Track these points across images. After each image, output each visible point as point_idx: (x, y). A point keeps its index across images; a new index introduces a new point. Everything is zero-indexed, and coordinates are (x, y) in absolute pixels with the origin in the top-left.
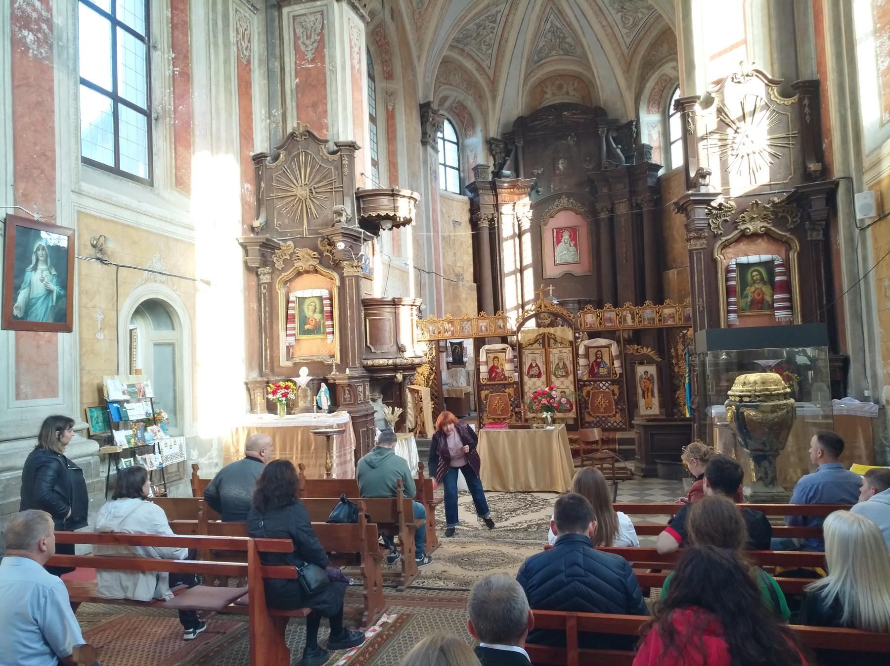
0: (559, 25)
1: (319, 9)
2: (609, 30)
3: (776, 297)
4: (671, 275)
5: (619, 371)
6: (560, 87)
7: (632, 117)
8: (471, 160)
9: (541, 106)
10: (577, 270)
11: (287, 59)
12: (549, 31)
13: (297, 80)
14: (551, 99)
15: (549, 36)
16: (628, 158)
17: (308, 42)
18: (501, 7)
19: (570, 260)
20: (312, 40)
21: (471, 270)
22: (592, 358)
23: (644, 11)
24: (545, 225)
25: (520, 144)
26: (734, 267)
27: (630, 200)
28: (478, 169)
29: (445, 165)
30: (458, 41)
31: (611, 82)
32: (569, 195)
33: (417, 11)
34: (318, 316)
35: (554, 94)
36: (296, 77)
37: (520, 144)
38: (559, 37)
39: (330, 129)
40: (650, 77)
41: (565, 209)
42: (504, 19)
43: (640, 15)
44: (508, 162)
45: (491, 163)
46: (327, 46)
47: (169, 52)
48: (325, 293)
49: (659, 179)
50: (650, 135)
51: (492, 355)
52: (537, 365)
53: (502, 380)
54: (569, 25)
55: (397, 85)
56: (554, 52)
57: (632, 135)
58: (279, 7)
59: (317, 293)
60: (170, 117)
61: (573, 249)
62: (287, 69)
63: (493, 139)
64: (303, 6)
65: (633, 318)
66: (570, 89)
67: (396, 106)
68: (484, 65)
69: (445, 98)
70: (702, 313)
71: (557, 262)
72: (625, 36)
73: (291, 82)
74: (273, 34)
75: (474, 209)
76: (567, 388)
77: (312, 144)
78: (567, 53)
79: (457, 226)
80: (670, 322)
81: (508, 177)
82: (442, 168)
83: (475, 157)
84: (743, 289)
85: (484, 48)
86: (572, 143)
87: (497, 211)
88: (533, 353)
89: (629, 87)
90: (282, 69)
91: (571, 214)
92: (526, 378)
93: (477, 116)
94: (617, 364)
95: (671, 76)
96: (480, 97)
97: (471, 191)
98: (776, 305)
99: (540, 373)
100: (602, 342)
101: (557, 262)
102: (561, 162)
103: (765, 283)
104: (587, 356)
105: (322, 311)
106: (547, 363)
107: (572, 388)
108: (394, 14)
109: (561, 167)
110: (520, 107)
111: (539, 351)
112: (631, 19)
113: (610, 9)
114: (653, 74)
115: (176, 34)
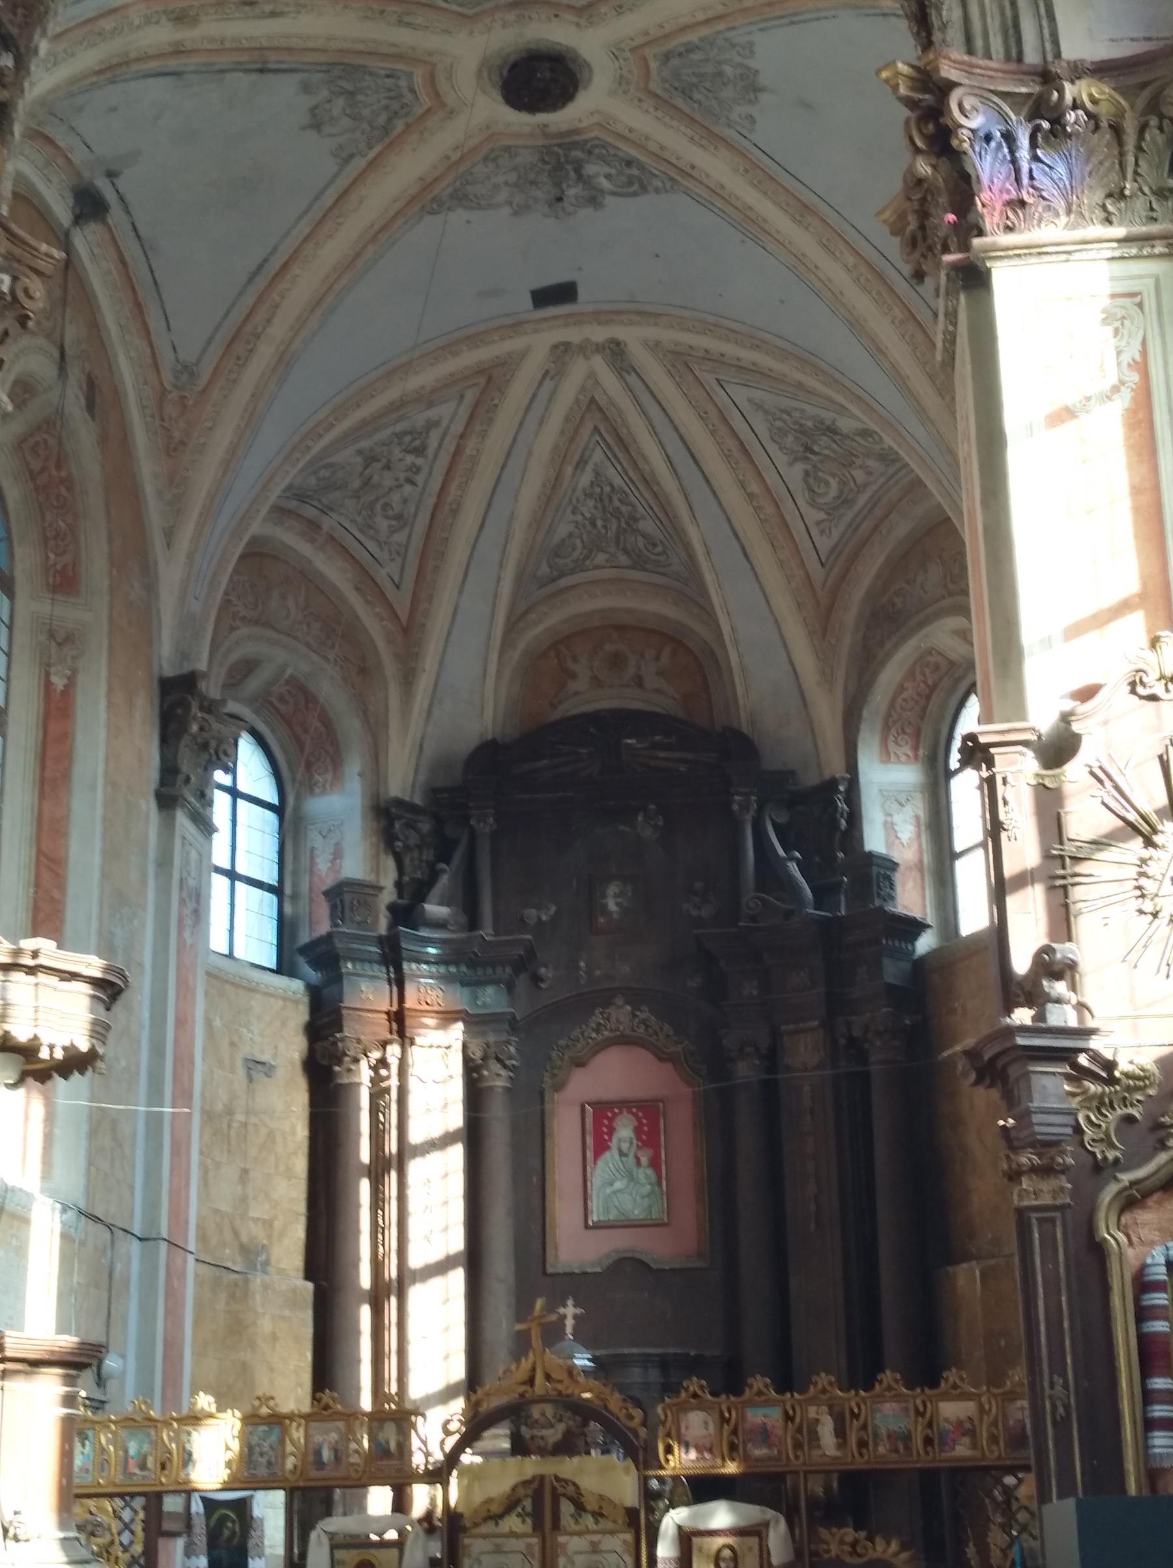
4: (961, 1281)
6: (617, 662)
8: (323, 865)
9: (557, 715)
10: (661, 1249)
12: (588, 495)
14: (586, 697)
15: (588, 508)
16: (823, 894)
18: (443, 411)
19: (637, 1213)
21: (299, 1231)
23: (872, 463)
24: (559, 1087)
25: (486, 826)
28: (344, 897)
29: (232, 875)
30: (299, 494)
33: (175, 395)
35: (597, 682)
37: (486, 826)
38: (617, 514)
41: (623, 1040)
42: (450, 446)
43: (859, 475)
44: (444, 880)
45: (388, 878)
49: (920, 965)
50: (890, 827)
54: (649, 481)
55: (91, 612)
56: (601, 558)
57: (834, 823)
61: (645, 1174)
63: (399, 802)
67: (81, 679)
69: (247, 667)
71: (594, 1217)
78: (639, 563)
79: (258, 1076)
80: (962, 1450)
81: (440, 925)
82: (220, 884)
83: (337, 854)
85: (383, 524)
86: (648, 833)
91: (643, 1056)
95: (954, 656)
97: (315, 964)
101: (594, 1217)
108: (99, 396)
109: (612, 906)
110: (489, 712)
112: (833, 483)
113: (772, 448)
114: (897, 646)
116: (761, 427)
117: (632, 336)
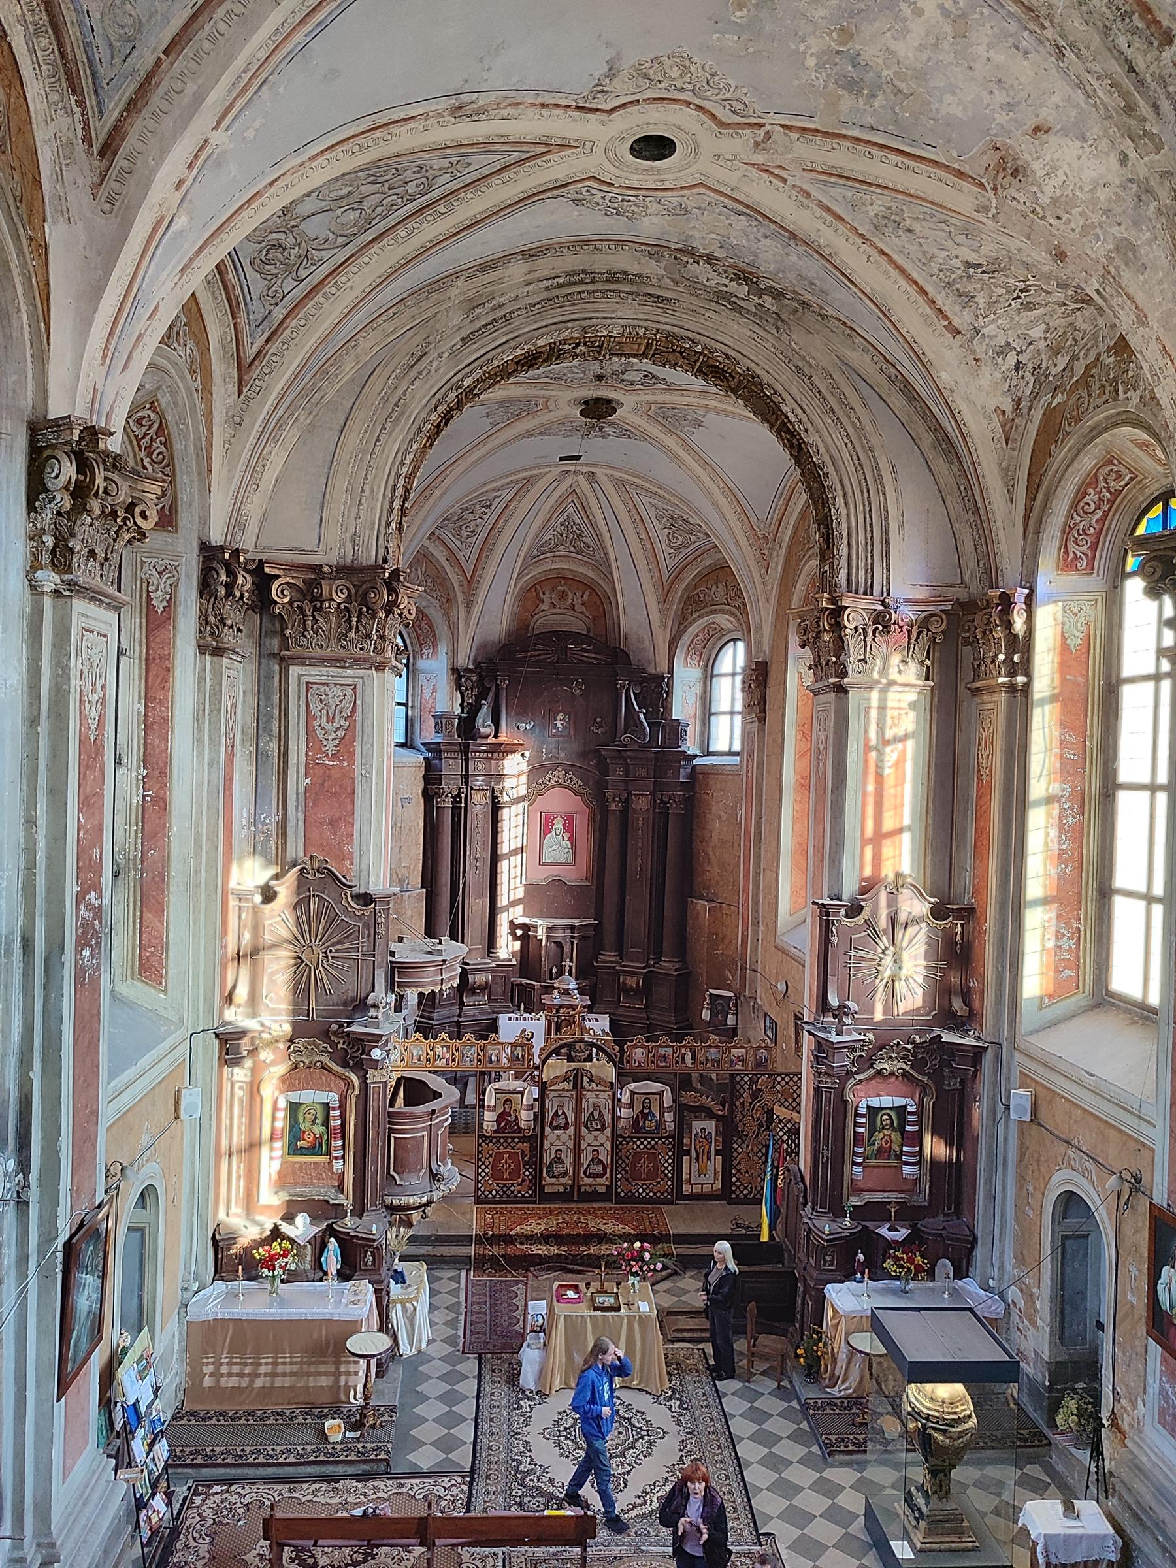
0: (577, 521)
1: (350, 681)
2: (649, 546)
3: (905, 1148)
5: (670, 1126)
6: (563, 596)
7: (663, 668)
11: (292, 746)
13: (308, 781)
17: (328, 727)
19: (562, 860)
20: (336, 725)
22: (638, 1108)
26: (864, 1110)
27: (653, 794)
31: (639, 612)
32: (567, 768)
34: (319, 1130)
36: (306, 775)
39: (356, 861)
40: (694, 621)
41: (561, 786)
46: (358, 739)
47: (139, 767)
48: (333, 1099)
51: (504, 1097)
52: (564, 1113)
53: (514, 1132)
58: (285, 662)
59: (323, 1097)
60: (135, 869)
62: (292, 760)
64: (324, 671)
65: (693, 1058)
66: (578, 602)
68: (460, 555)
70: (825, 1164)
72: (667, 557)
73: (297, 782)
74: (268, 698)
75: (432, 777)
76: (602, 1145)
77: (331, 886)
78: (579, 552)
84: (871, 1135)
87: (467, 784)
88: (560, 1096)
89: (664, 625)
90: (284, 754)
92: (547, 1129)
93: (442, 629)
94: (669, 1117)
96: (448, 601)
98: (905, 1158)
99: (567, 1123)
100: (656, 1086)
102: (560, 717)
103: (894, 1130)
104: (630, 1106)
105: (326, 1123)
106: (578, 1110)
107: (608, 1145)
109: (559, 725)
110: (504, 622)
111: (568, 1094)
115: (150, 738)
116: (652, 513)
117: (600, 473)
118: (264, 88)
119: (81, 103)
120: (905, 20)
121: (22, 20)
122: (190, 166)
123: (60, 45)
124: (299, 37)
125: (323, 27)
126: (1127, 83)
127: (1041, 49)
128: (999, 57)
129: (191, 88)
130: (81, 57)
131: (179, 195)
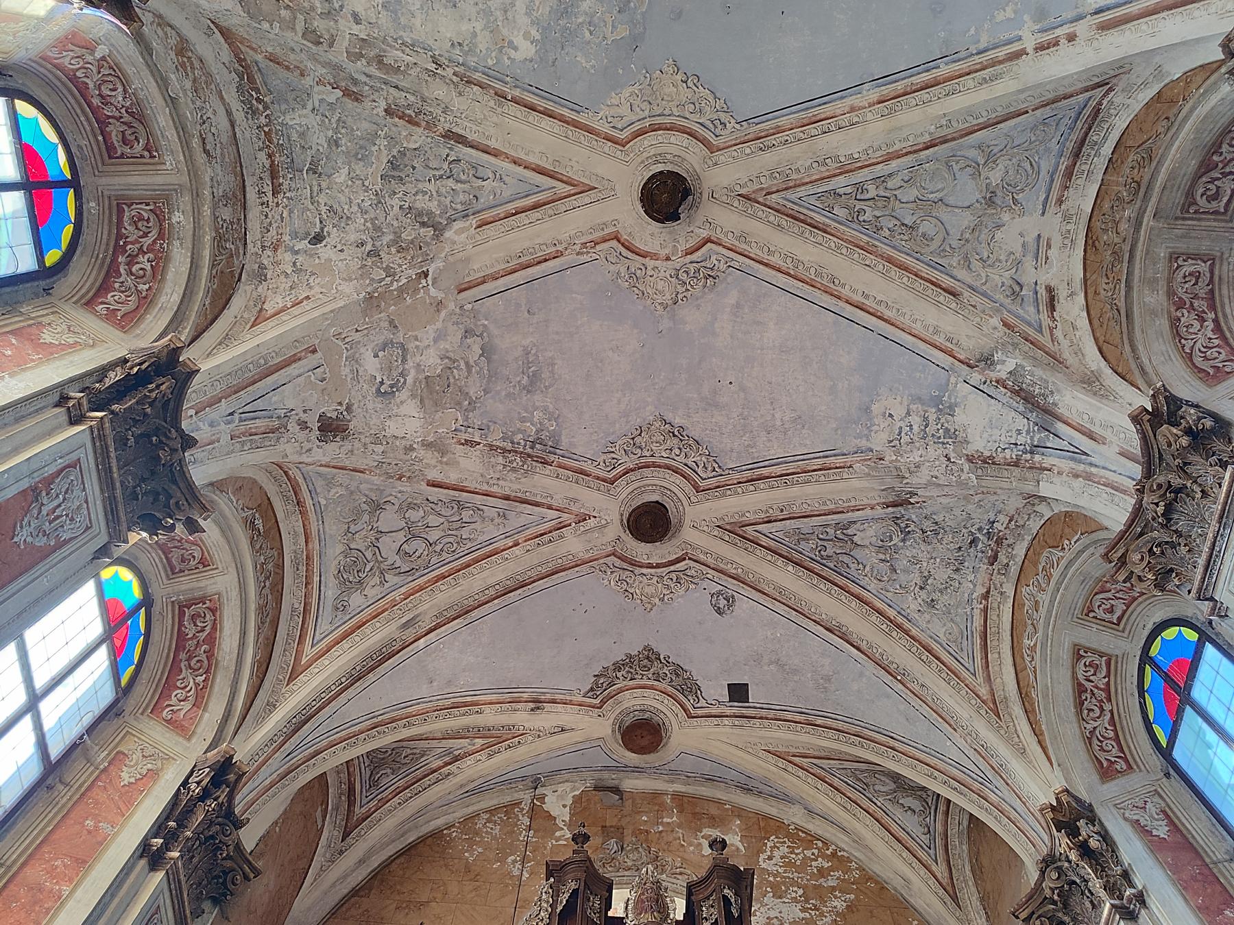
118: (982, 46)
119: (1100, 103)
120: (533, 23)
121: (1098, 154)
122: (1057, 44)
123: (1087, 134)
124: (944, 70)
125: (929, 65)
126: (394, 79)
127: (446, 55)
128: (465, 27)
129: (1022, 96)
130: (1079, 124)
131: (1081, 28)
